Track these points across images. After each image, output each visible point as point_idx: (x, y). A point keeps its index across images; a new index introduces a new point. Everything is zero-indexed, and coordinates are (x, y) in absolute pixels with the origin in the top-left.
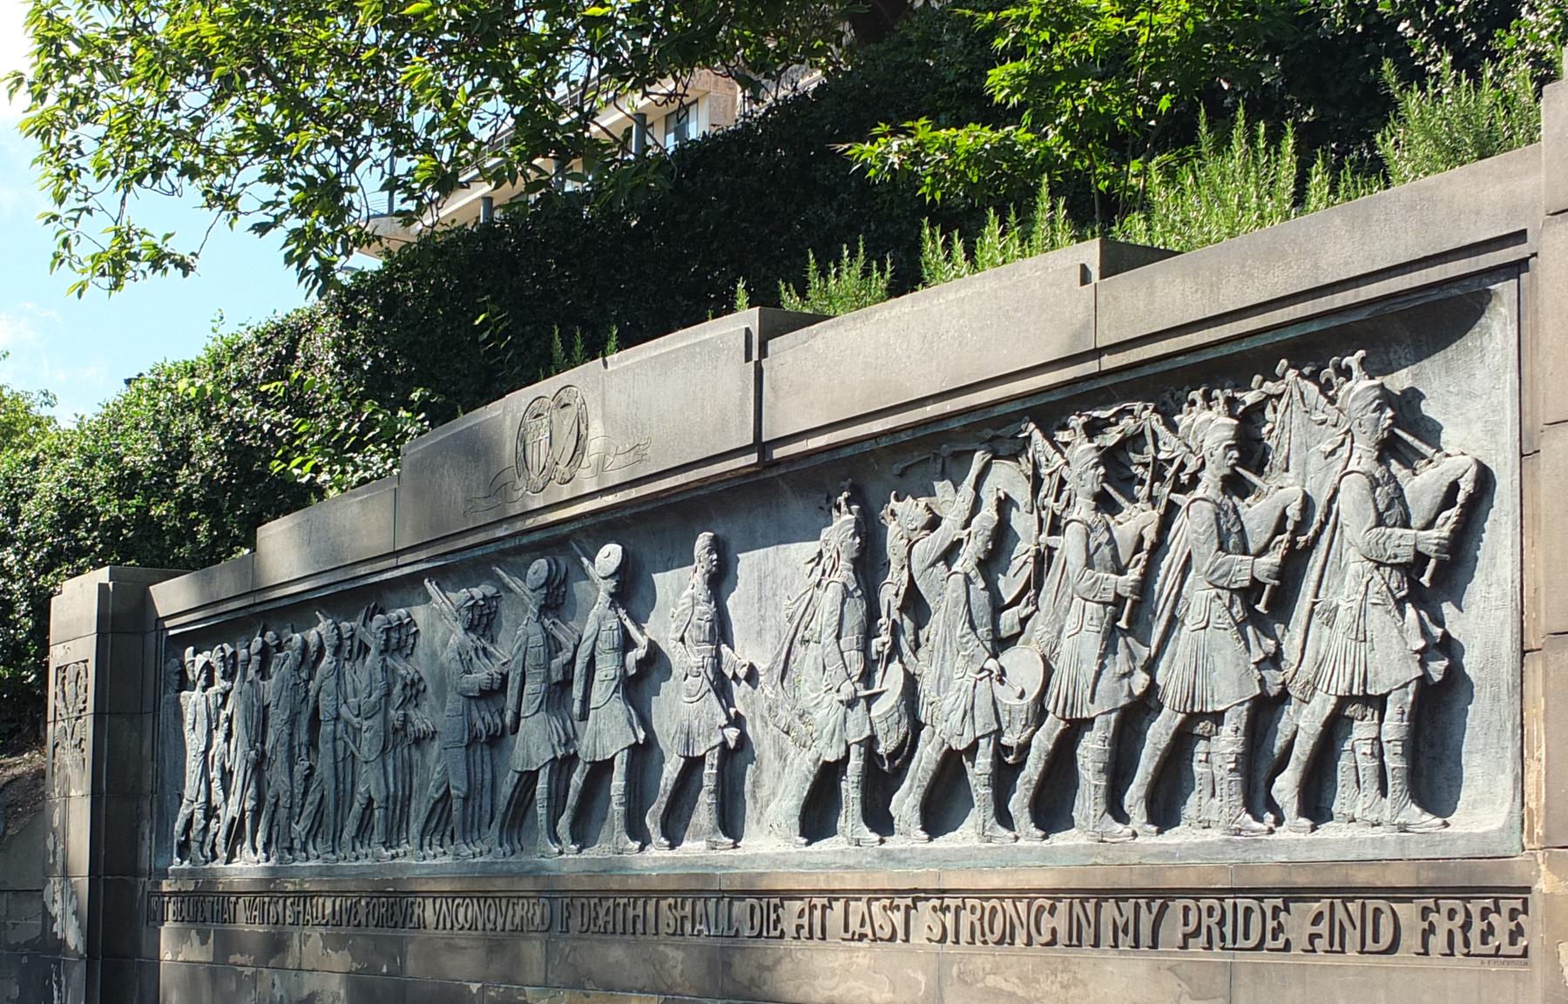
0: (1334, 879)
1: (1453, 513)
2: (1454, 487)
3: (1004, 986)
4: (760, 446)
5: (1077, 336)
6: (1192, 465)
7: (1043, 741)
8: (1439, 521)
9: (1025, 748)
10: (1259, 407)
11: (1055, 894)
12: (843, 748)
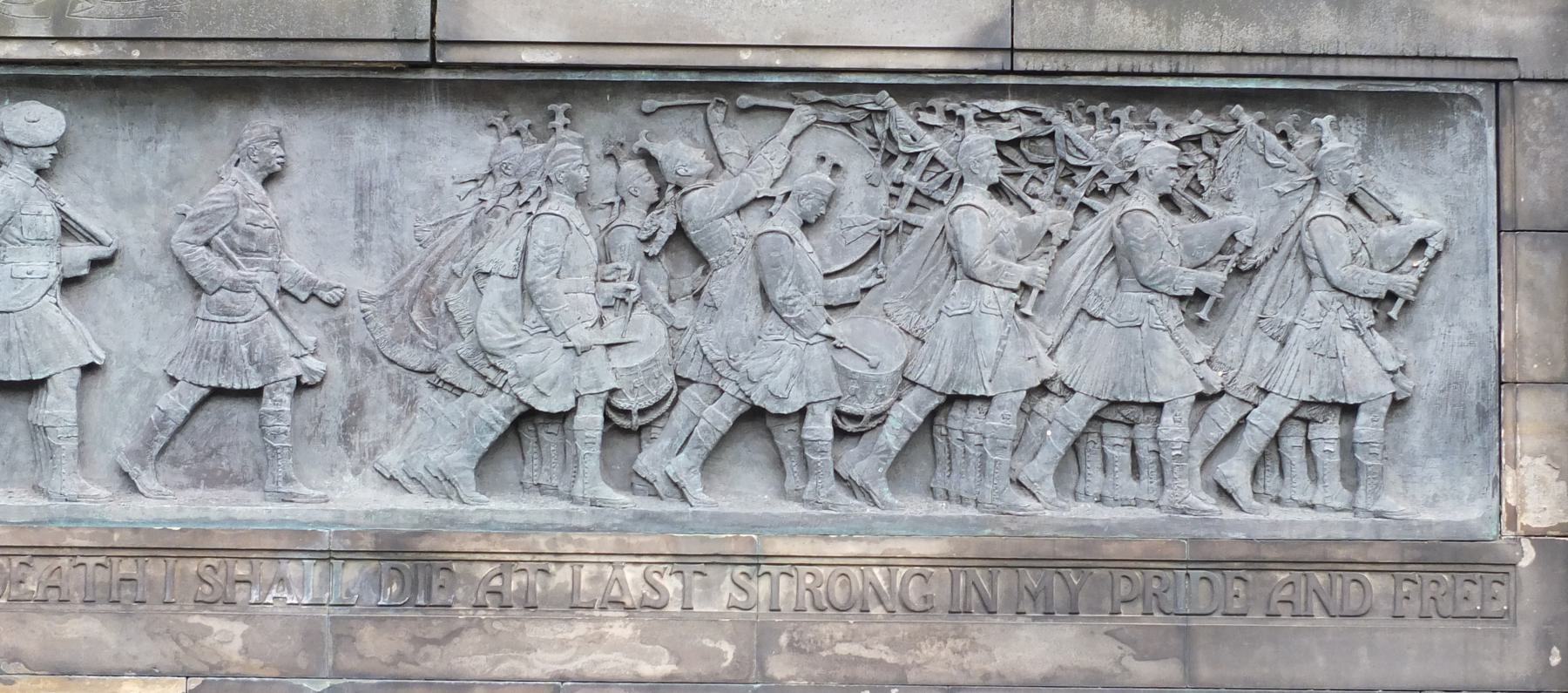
0: (1312, 553)
1: (1421, 263)
2: (1422, 244)
3: (865, 653)
5: (990, 28)
6: (1117, 174)
7: (908, 412)
8: (1404, 268)
9: (881, 417)
10: (1197, 140)
11: (936, 561)
12: (572, 398)
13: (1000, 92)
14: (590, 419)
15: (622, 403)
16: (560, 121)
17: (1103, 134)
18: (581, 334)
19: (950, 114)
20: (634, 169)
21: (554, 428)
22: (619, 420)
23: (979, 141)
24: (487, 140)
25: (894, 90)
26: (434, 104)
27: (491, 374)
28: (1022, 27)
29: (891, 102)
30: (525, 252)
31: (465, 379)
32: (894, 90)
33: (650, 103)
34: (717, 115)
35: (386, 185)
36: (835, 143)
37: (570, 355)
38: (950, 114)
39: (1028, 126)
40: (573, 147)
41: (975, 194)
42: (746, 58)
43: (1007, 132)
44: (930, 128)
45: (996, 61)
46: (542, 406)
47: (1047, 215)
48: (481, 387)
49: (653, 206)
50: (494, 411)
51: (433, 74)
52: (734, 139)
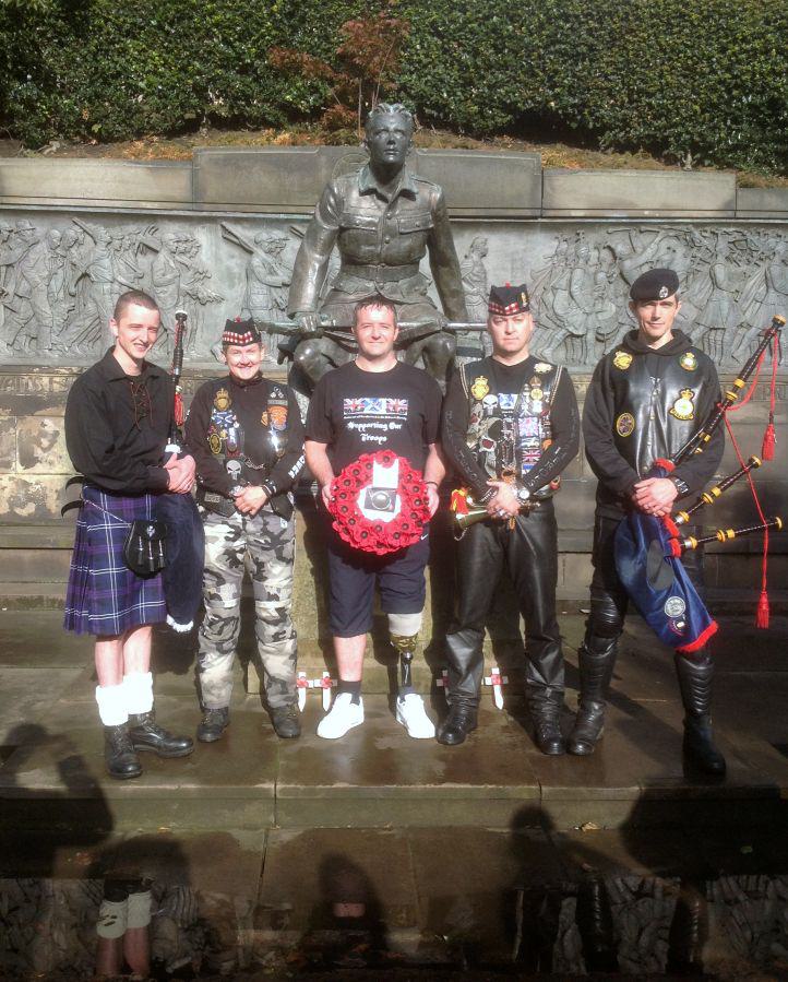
4: (542, 208)
6: (767, 253)
13: (729, 225)
14: (591, 336)
15: (600, 331)
16: (581, 236)
17: (762, 240)
18: (587, 309)
19: (713, 233)
20: (606, 254)
21: (579, 340)
22: (600, 337)
23: (722, 244)
24: (556, 243)
25: (696, 225)
26: (538, 231)
27: (558, 322)
28: (739, 202)
29: (691, 228)
30: (570, 281)
31: (550, 324)
32: (696, 225)
33: (610, 230)
34: (634, 233)
35: (521, 259)
36: (673, 243)
37: (585, 316)
38: (713, 233)
39: (739, 237)
40: (589, 246)
41: (721, 259)
42: (646, 213)
43: (731, 239)
44: (704, 237)
45: (730, 214)
46: (575, 332)
47: (744, 268)
48: (554, 326)
49: (611, 265)
50: (560, 334)
51: (540, 220)
52: (641, 240)
